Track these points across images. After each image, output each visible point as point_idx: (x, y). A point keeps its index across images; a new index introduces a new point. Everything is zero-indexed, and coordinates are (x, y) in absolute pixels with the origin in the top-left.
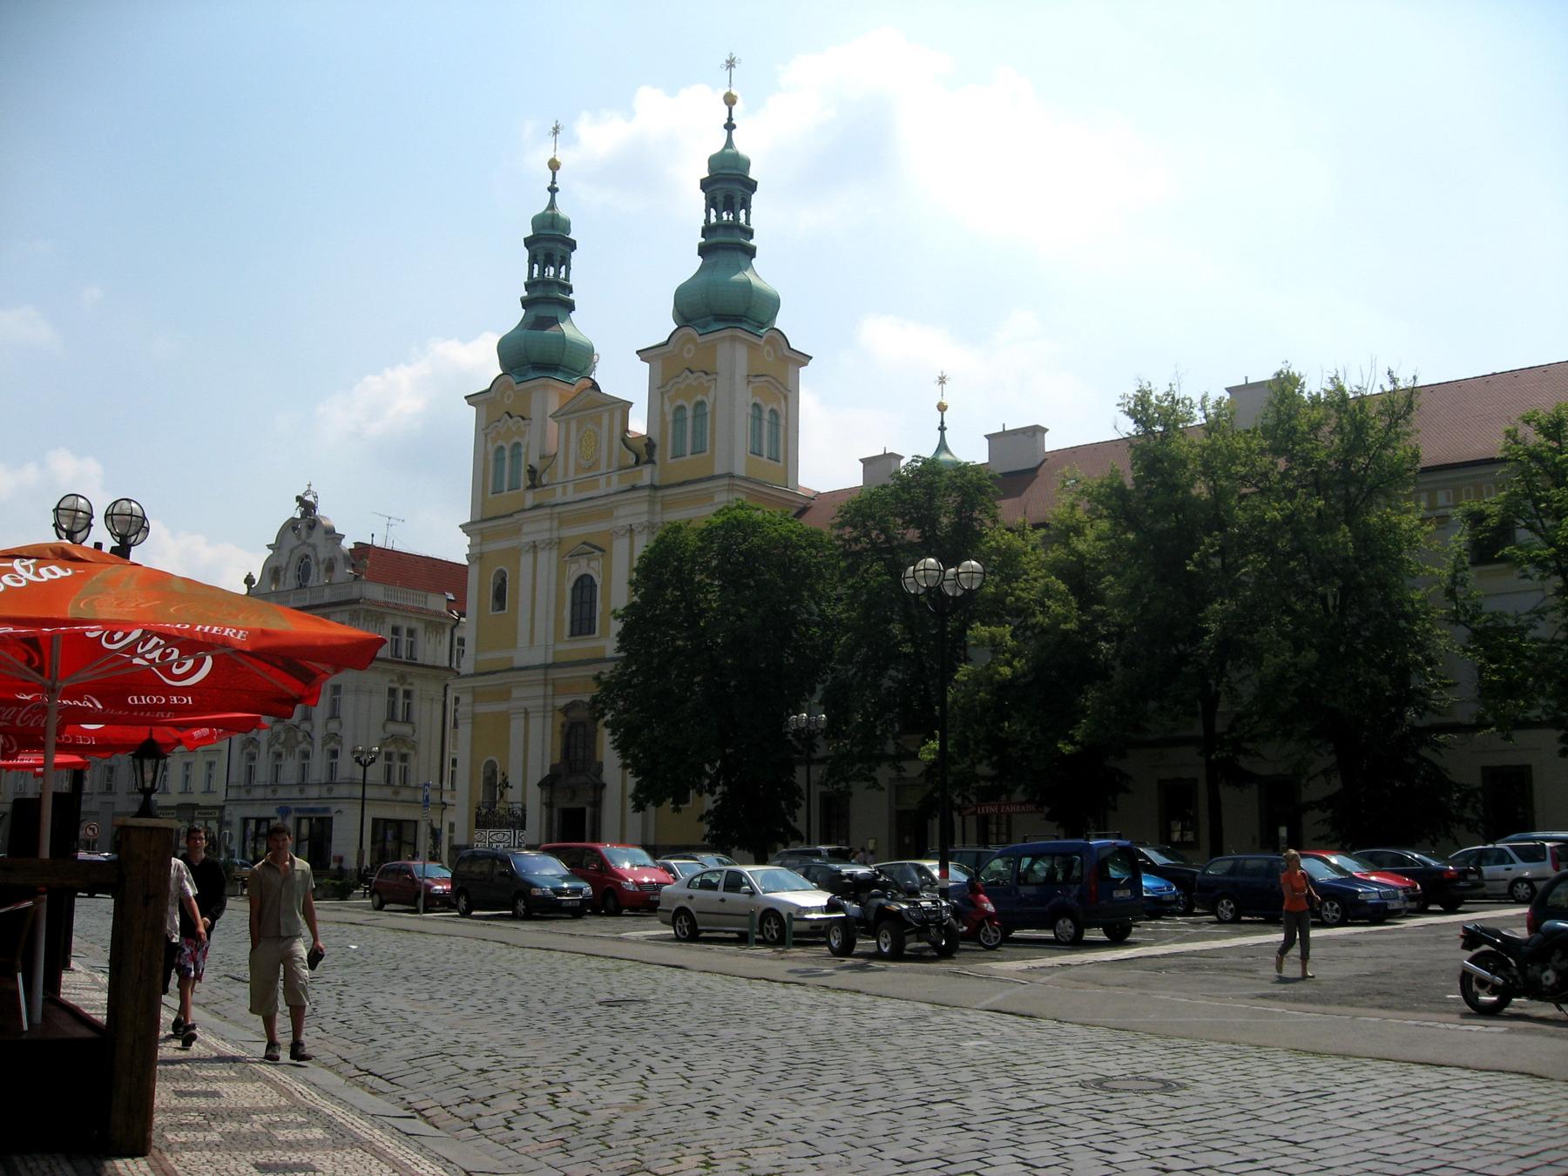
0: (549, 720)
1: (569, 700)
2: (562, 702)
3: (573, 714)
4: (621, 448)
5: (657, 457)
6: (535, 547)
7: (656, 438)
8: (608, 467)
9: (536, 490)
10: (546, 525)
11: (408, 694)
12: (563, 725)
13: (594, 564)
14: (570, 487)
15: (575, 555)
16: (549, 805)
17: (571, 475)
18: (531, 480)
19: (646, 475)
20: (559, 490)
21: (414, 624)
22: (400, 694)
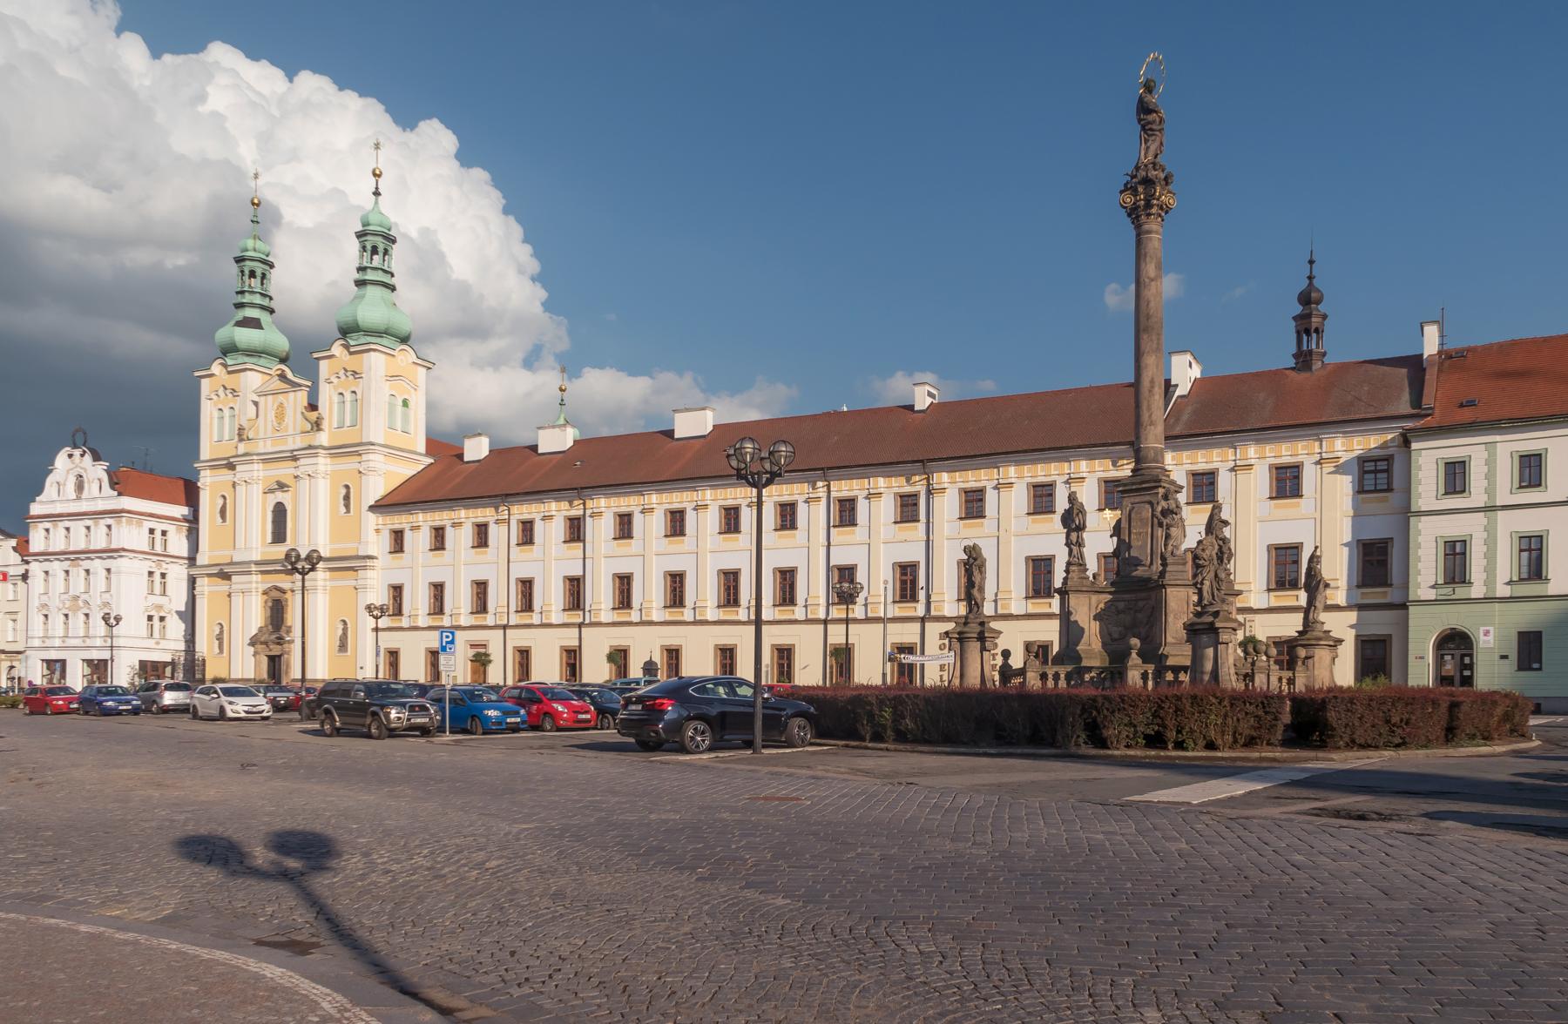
11: (163, 575)
12: (266, 602)
14: (269, 442)
15: (271, 491)
20: (261, 443)
21: (164, 527)
22: (157, 577)
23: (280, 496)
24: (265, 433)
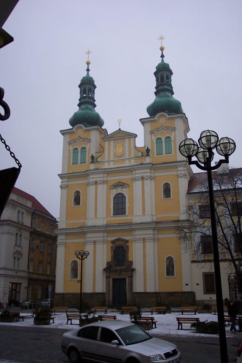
0: (105, 245)
1: (116, 238)
2: (113, 239)
3: (117, 243)
5: (150, 154)
6: (96, 183)
7: (150, 148)
8: (129, 157)
10: (102, 175)
12: (112, 247)
13: (124, 190)
15: (115, 186)
16: (108, 277)
18: (92, 160)
19: (148, 160)
20: (106, 164)
23: (119, 190)
24: (109, 158)
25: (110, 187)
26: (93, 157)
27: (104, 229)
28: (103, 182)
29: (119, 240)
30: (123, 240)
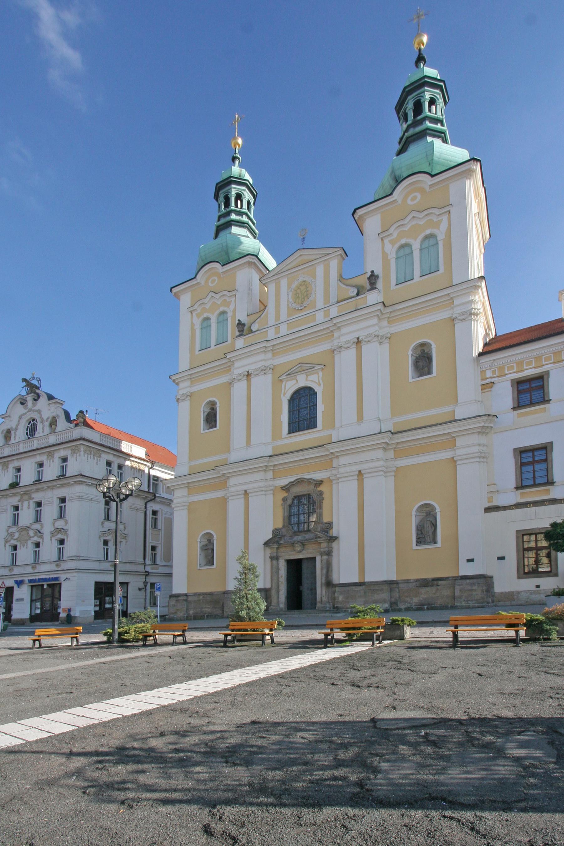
1: (292, 479)
2: (285, 482)
4: (338, 284)
9: (246, 337)
17: (284, 316)
18: (239, 331)
25: (280, 378)
26: (240, 325)
27: (266, 464)
28: (264, 370)
29: (300, 481)
30: (309, 481)
